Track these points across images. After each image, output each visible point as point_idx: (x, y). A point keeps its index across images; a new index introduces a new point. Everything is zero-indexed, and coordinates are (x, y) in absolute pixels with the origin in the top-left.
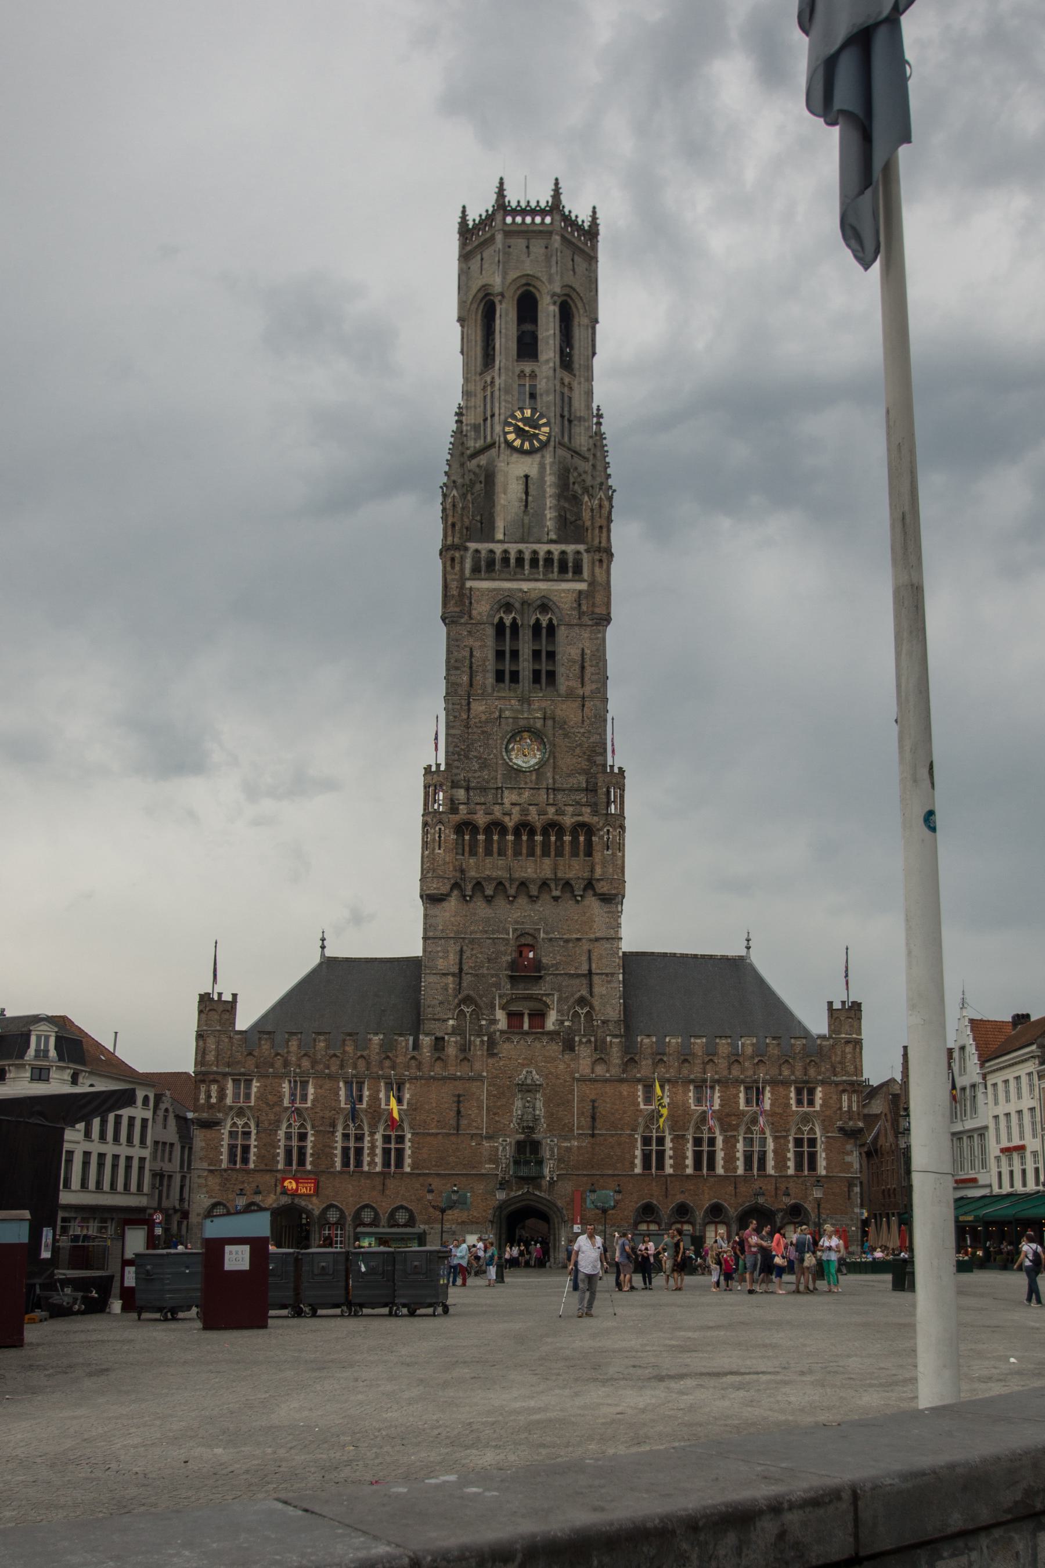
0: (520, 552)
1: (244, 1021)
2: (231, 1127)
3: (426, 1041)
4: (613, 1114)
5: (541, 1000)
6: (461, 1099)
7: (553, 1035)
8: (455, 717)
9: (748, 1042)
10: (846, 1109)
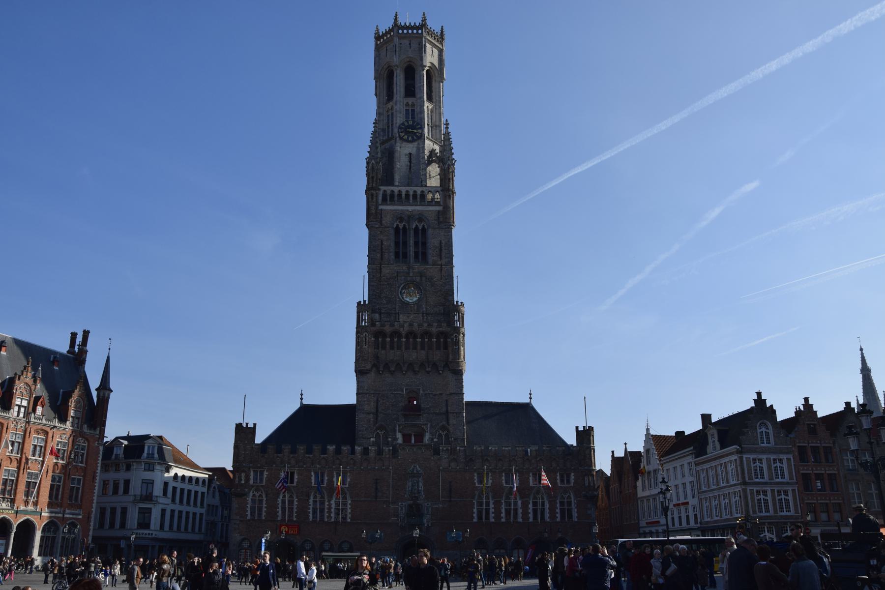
1: (259, 438)
8: (373, 276)
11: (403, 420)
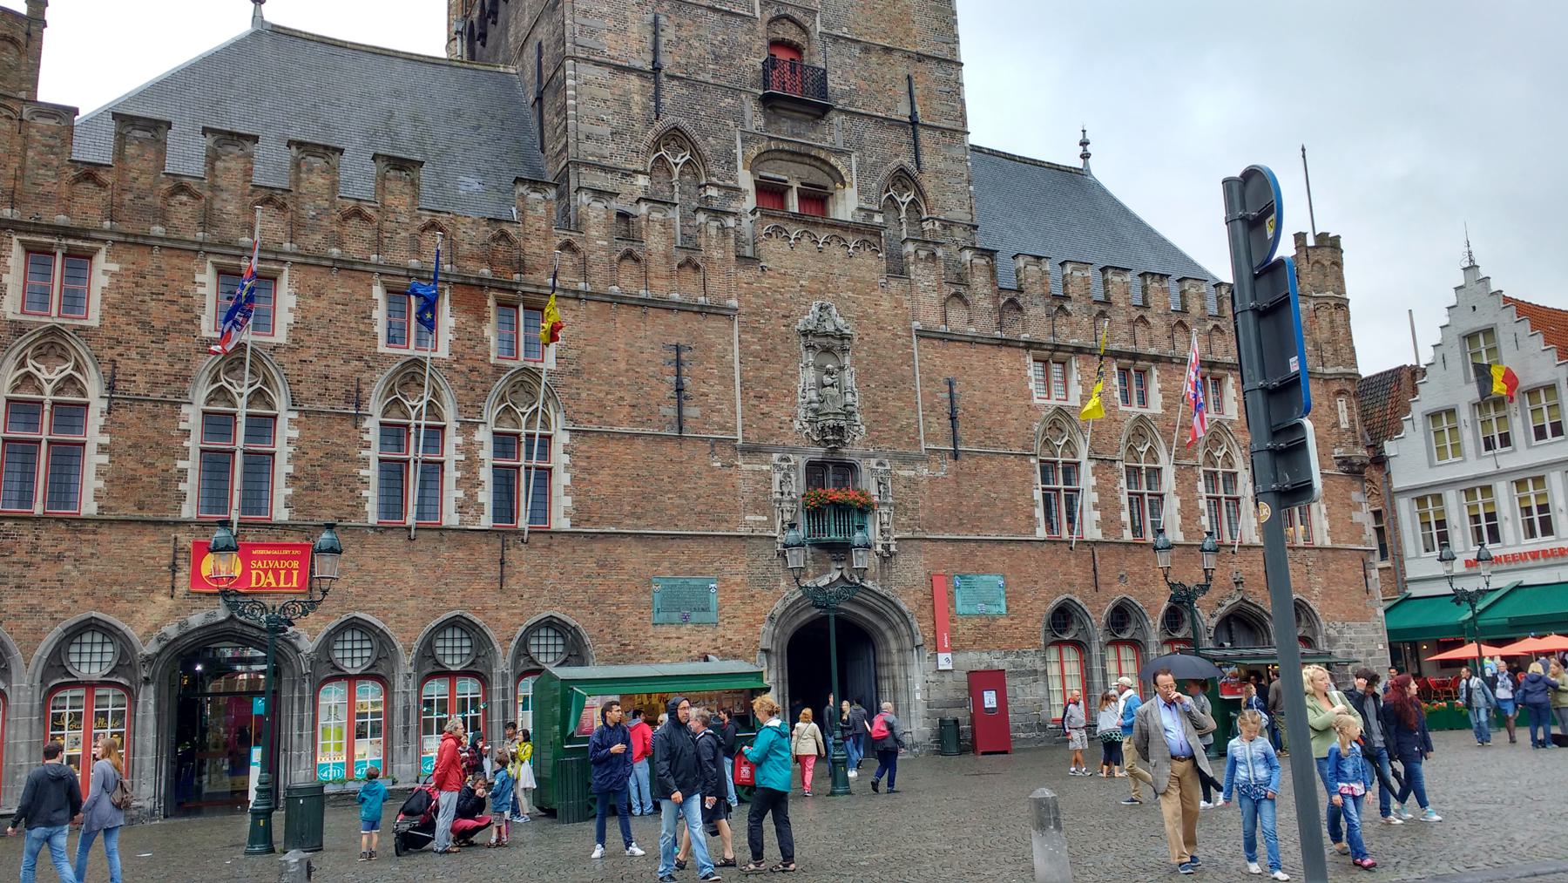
2: (15, 389)
4: (988, 412)
6: (684, 356)
7: (866, 233)
9: (1193, 290)
10: (1344, 426)
11: (761, 123)
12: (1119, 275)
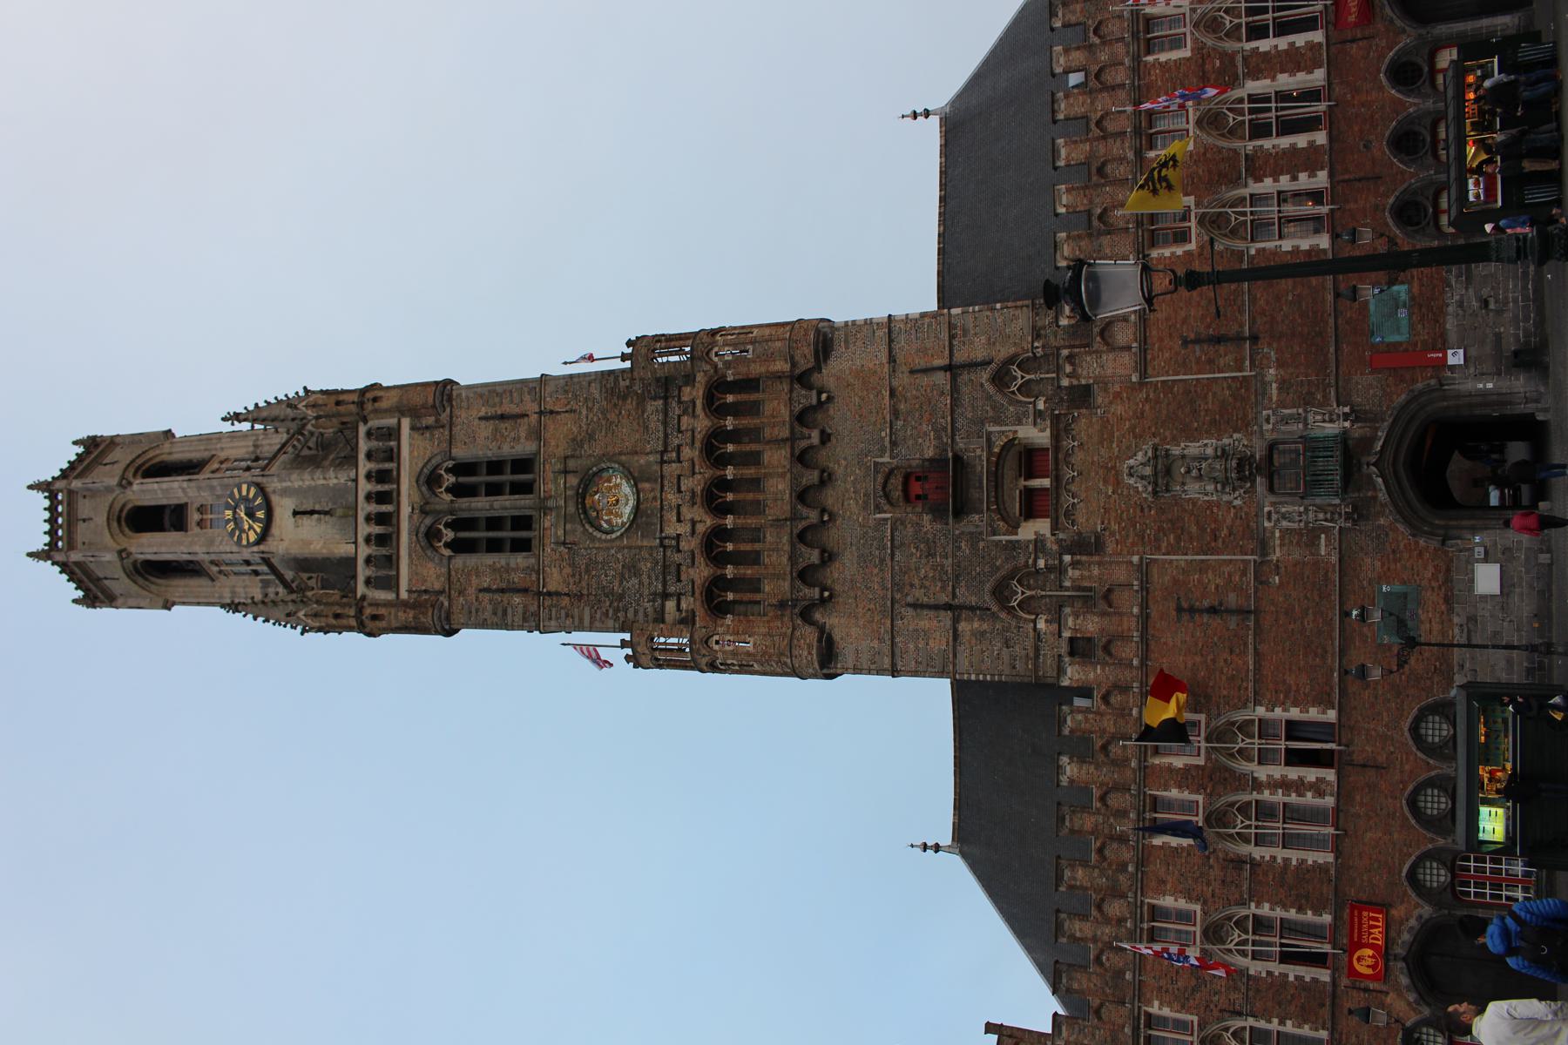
0: (368, 519)
3: (1073, 674)
5: (998, 458)
6: (1185, 605)
7: (1060, 429)
9: (1062, 60)
12: (1059, 152)
